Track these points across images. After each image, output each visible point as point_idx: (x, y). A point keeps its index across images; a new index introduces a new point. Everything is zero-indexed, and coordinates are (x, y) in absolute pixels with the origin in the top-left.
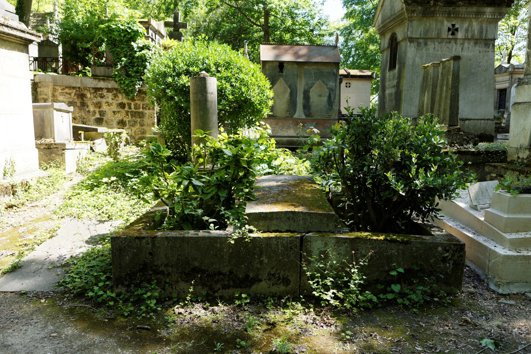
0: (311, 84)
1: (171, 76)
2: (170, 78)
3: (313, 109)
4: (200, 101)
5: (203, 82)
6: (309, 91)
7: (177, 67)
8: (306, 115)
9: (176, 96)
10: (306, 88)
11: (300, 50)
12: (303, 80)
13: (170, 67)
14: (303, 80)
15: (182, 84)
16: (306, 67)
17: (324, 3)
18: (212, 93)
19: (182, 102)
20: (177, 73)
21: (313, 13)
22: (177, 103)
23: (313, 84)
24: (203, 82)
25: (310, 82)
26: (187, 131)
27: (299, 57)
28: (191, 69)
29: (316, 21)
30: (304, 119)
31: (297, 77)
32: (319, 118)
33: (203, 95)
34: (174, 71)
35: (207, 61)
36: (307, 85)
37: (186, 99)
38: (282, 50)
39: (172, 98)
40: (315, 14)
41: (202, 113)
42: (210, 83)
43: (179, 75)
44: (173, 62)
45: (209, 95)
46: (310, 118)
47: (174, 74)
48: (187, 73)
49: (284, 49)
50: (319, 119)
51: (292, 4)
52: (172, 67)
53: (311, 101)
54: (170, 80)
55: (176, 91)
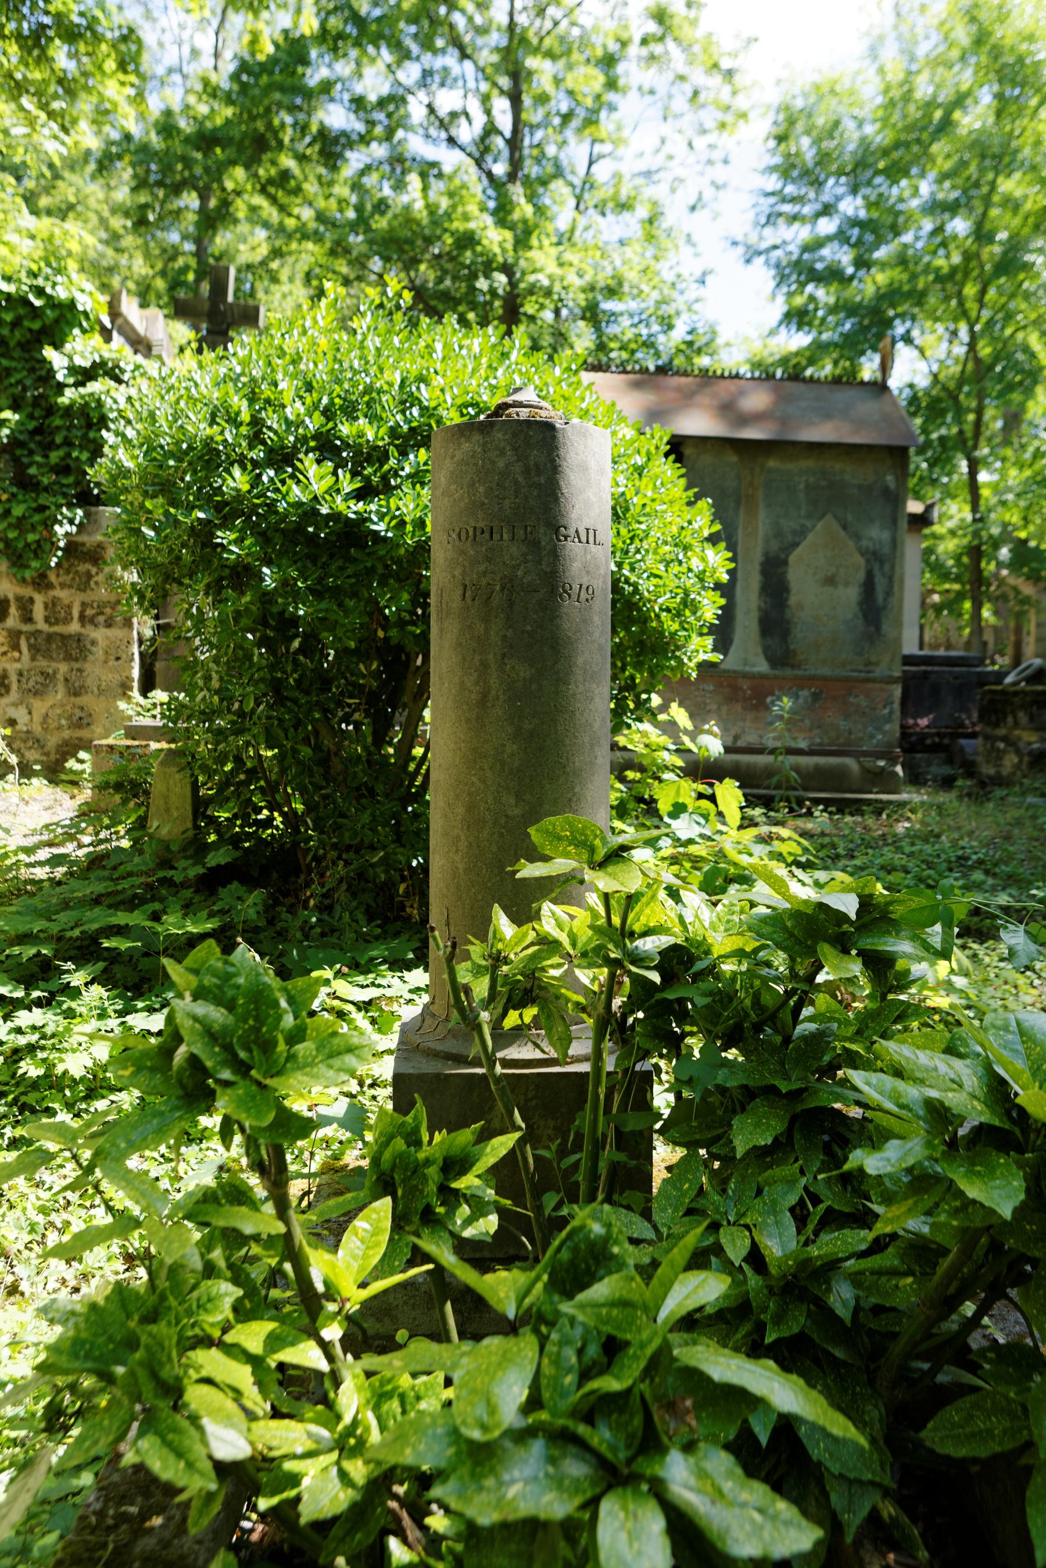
0: (794, 533)
1: (242, 461)
2: (236, 471)
3: (801, 636)
4: (509, 585)
5: (535, 456)
6: (785, 563)
7: (272, 420)
8: (774, 661)
9: (269, 563)
10: (775, 546)
11: (742, 393)
12: (762, 513)
13: (234, 421)
14: (762, 513)
15: (299, 504)
16: (772, 463)
17: (708, 279)
18: (591, 536)
19: (297, 596)
20: (270, 451)
21: (670, 310)
22: (266, 598)
23: (802, 533)
26: (306, 741)
27: (744, 420)
28: (345, 429)
29: (679, 334)
30: (762, 676)
31: (738, 502)
32: (825, 671)
33: (535, 544)
34: (256, 439)
36: (779, 534)
37: (320, 580)
38: (671, 395)
39: (242, 575)
40: (678, 313)
41: (524, 671)
42: (585, 468)
43: (283, 458)
44: (252, 398)
45: (573, 549)
46: (788, 672)
48: (327, 447)
49: (679, 389)
50: (825, 679)
51: (603, 279)
52: (245, 416)
53: (793, 600)
54: (238, 480)
55: (264, 538)
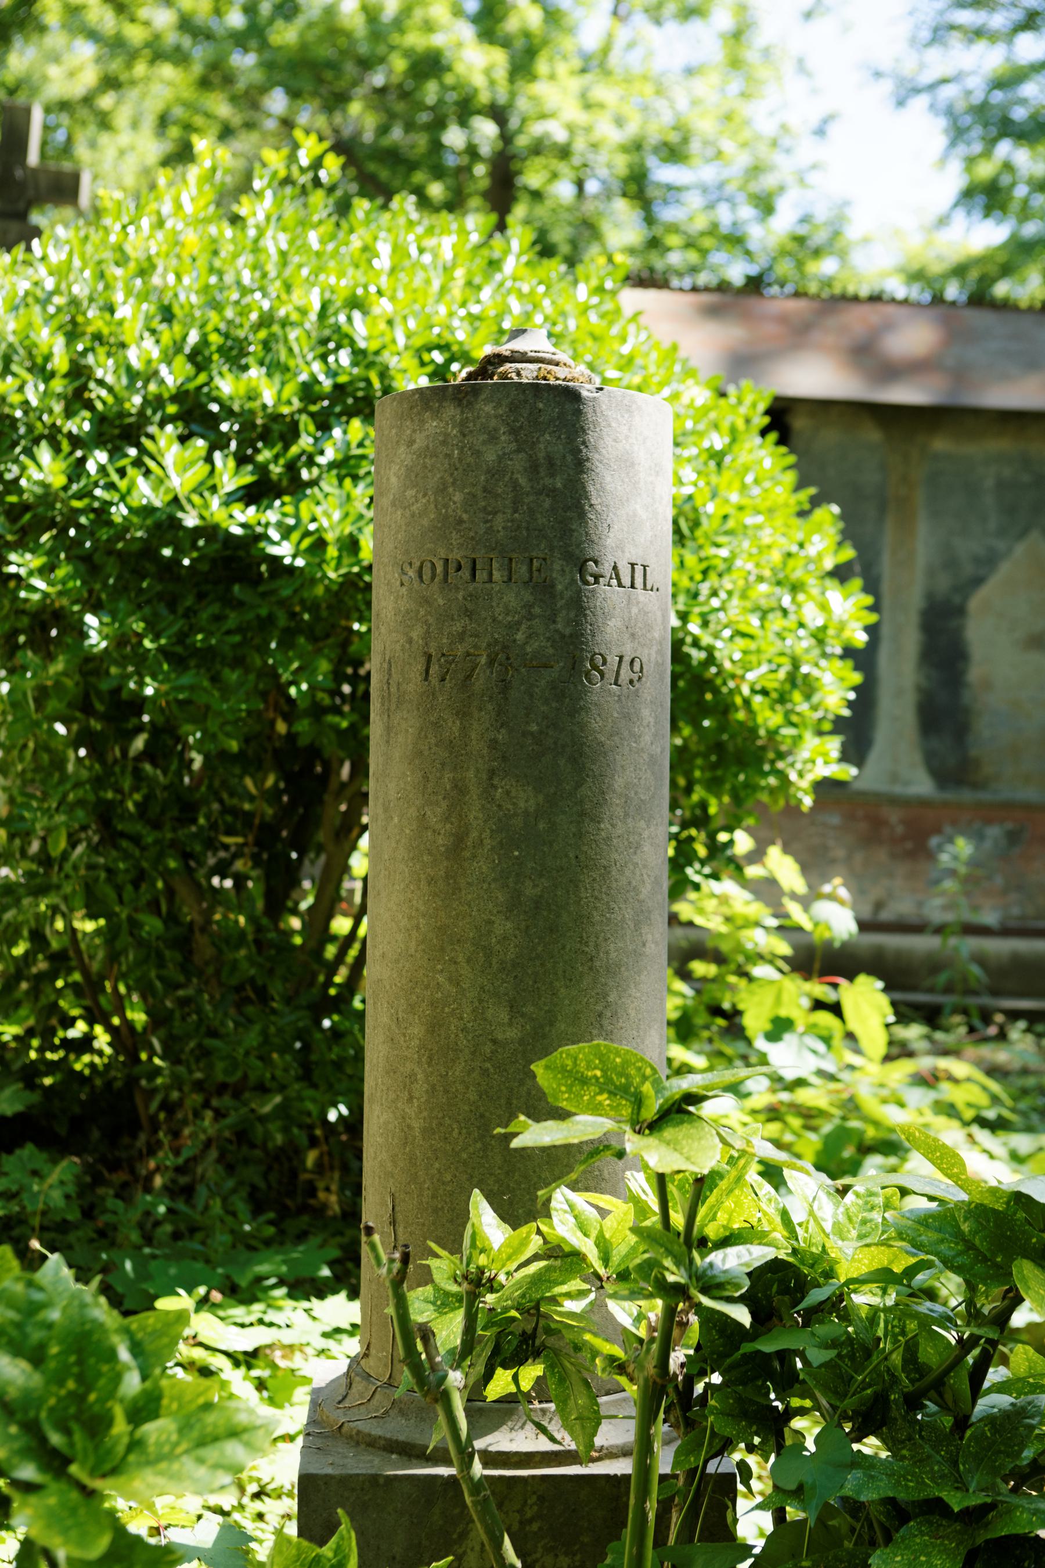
0: (977, 561)
1: (53, 437)
2: (44, 453)
3: (989, 733)
4: (503, 656)
5: (547, 443)
6: (961, 611)
7: (104, 368)
8: (942, 776)
9: (96, 608)
10: (944, 583)
11: (888, 326)
12: (923, 528)
13: (42, 371)
14: (923, 528)
15: (148, 510)
16: (941, 444)
17: (833, 129)
18: (638, 575)
19: (142, 663)
20: (101, 421)
21: (768, 182)
22: (91, 666)
23: (989, 561)
24: (547, 443)
25: (967, 547)
26: (154, 907)
27: (891, 371)
28: (227, 385)
29: (784, 221)
30: (923, 803)
31: (882, 508)
32: (1029, 794)
33: (545, 589)
34: (77, 400)
35: (360, 328)
36: (950, 563)
37: (182, 638)
38: (771, 329)
39: (49, 626)
40: (781, 189)
41: (526, 799)
42: (628, 463)
43: (121, 432)
44: (73, 333)
45: (608, 596)
46: (967, 796)
47: (82, 424)
48: (195, 415)
49: (783, 319)
50: (1028, 807)
51: (657, 129)
52: (60, 362)
53: (974, 674)
54: (45, 469)
55: (88, 565)
